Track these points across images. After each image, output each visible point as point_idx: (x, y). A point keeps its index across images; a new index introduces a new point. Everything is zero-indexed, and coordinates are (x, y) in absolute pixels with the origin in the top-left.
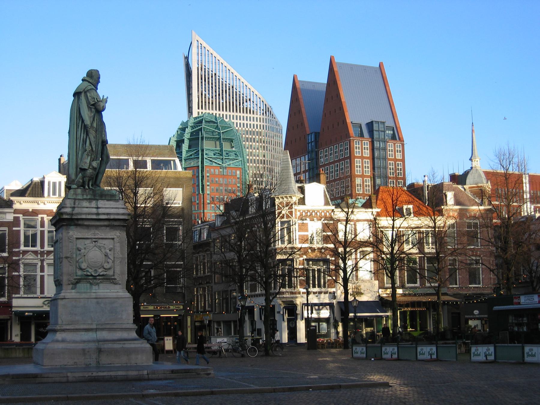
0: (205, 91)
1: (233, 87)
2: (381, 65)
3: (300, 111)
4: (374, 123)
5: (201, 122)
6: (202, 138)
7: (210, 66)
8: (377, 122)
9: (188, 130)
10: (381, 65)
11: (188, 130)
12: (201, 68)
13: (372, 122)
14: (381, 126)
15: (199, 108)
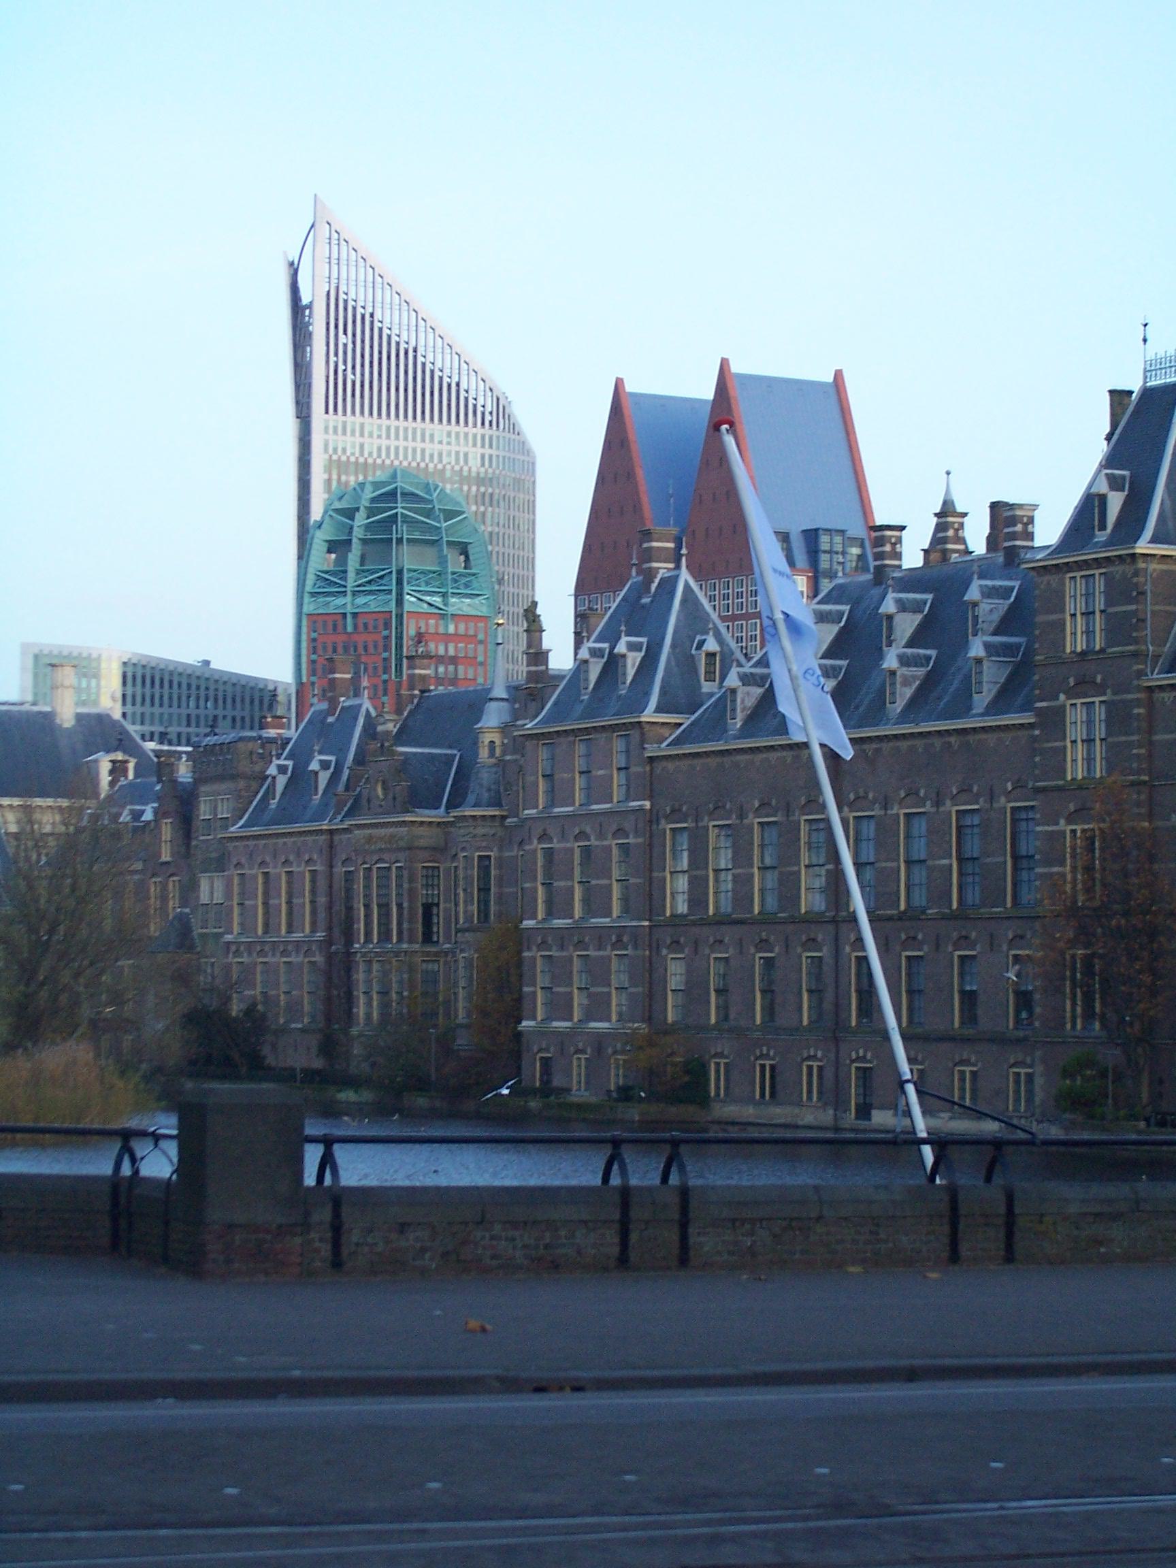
0: (336, 355)
1: (415, 351)
2: (838, 375)
3: (630, 475)
4: (821, 532)
5: (392, 495)
6: (399, 541)
7: (358, 294)
8: (828, 531)
9: (361, 519)
10: (838, 375)
11: (361, 519)
12: (334, 299)
13: (816, 530)
14: (838, 539)
15: (327, 412)
